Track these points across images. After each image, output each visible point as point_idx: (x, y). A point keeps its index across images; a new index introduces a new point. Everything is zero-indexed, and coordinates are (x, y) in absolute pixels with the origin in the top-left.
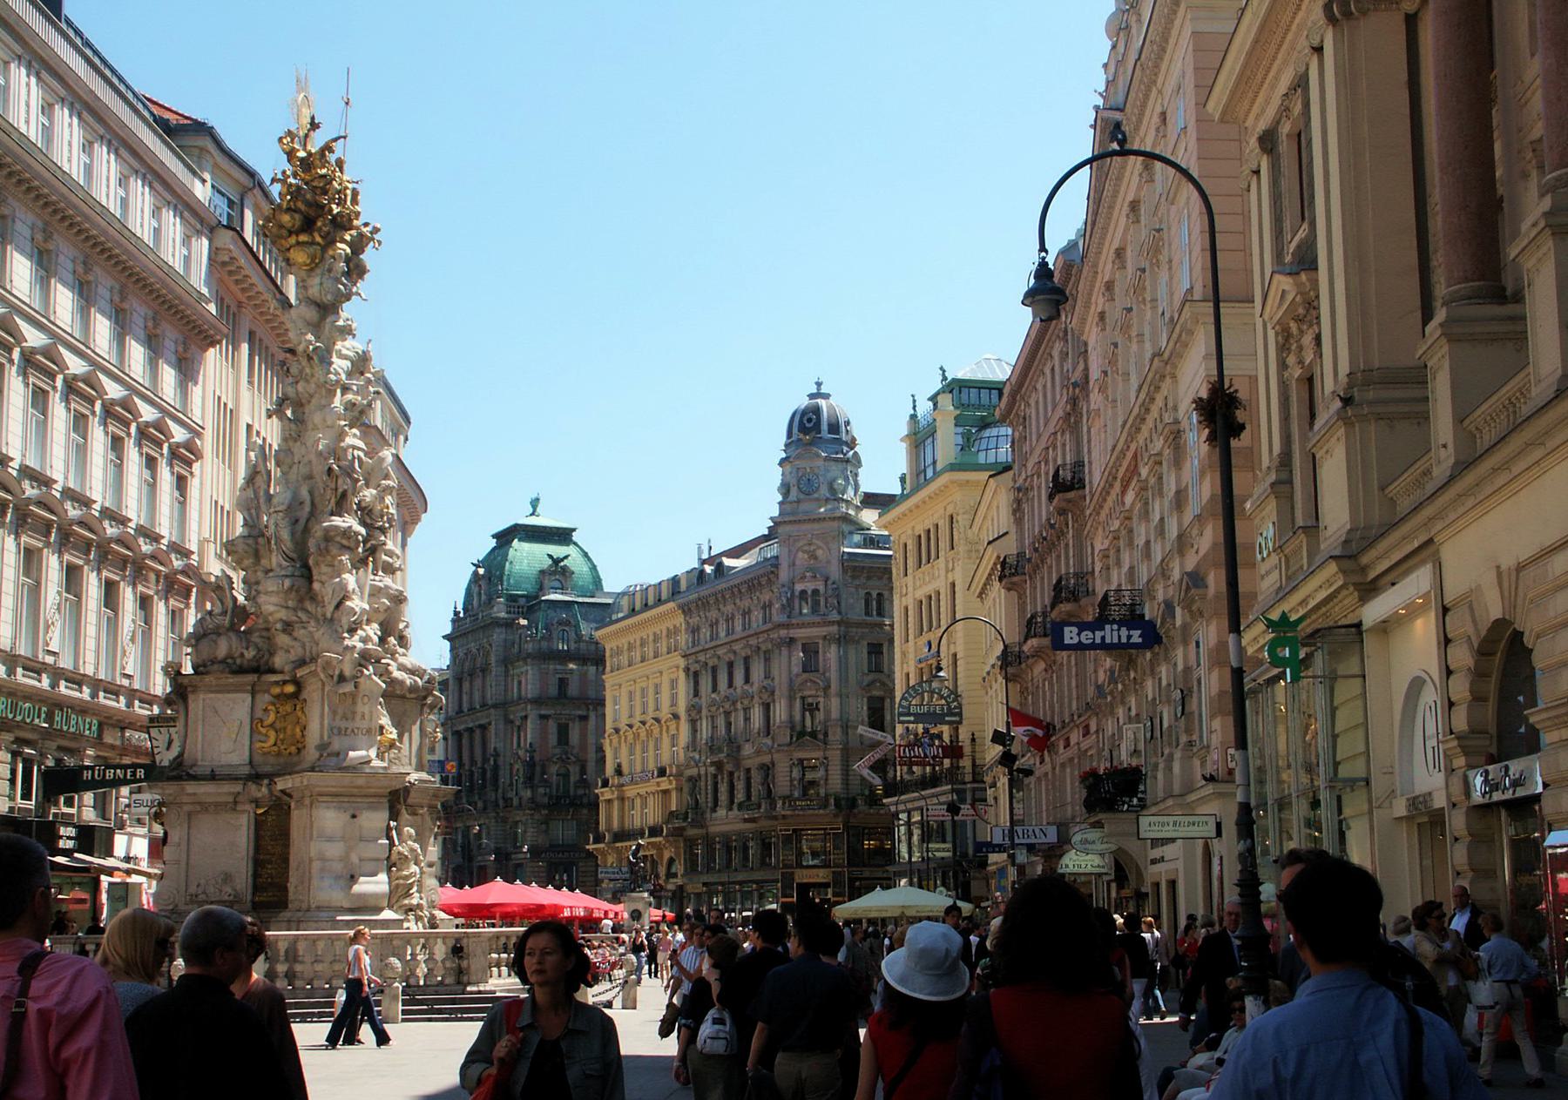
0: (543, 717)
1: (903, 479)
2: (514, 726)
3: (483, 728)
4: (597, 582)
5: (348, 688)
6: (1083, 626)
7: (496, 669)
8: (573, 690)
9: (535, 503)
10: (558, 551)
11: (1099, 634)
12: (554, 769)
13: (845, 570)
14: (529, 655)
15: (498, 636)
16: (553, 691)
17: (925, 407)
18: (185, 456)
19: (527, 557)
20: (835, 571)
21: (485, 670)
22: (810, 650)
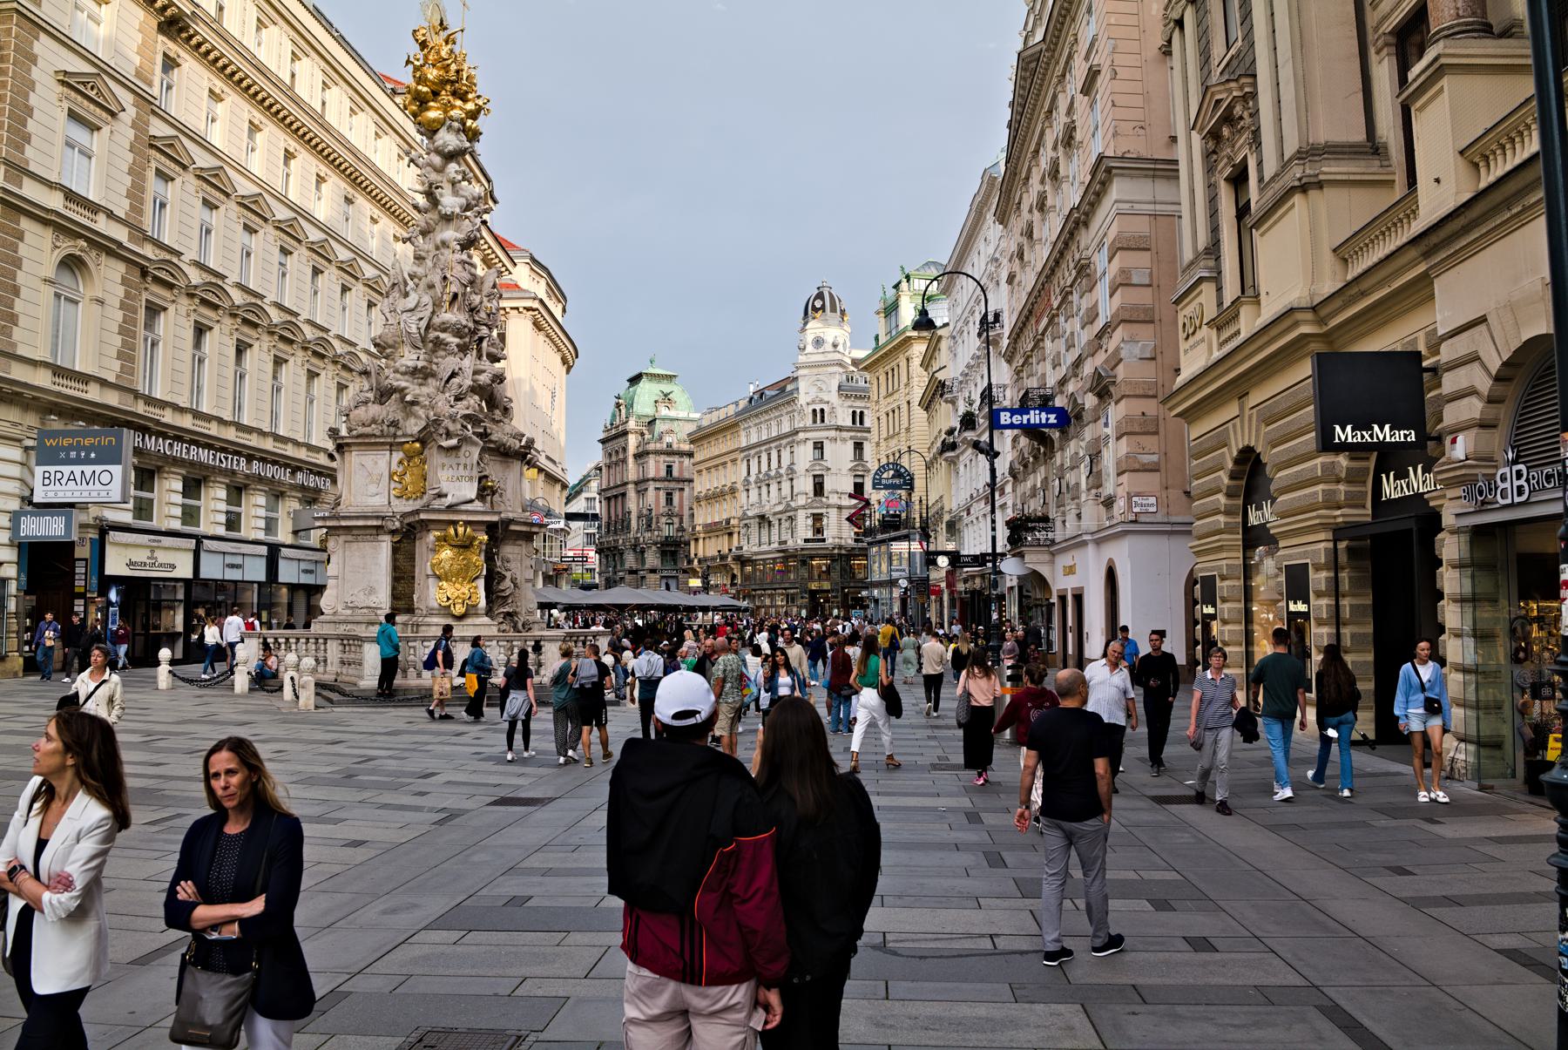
1: (877, 338)
2: (641, 492)
3: (624, 495)
6: (1013, 412)
7: (631, 460)
8: (675, 473)
10: (666, 387)
11: (1025, 417)
13: (840, 395)
16: (663, 473)
17: (891, 292)
20: (833, 397)
21: (624, 461)
22: (819, 446)
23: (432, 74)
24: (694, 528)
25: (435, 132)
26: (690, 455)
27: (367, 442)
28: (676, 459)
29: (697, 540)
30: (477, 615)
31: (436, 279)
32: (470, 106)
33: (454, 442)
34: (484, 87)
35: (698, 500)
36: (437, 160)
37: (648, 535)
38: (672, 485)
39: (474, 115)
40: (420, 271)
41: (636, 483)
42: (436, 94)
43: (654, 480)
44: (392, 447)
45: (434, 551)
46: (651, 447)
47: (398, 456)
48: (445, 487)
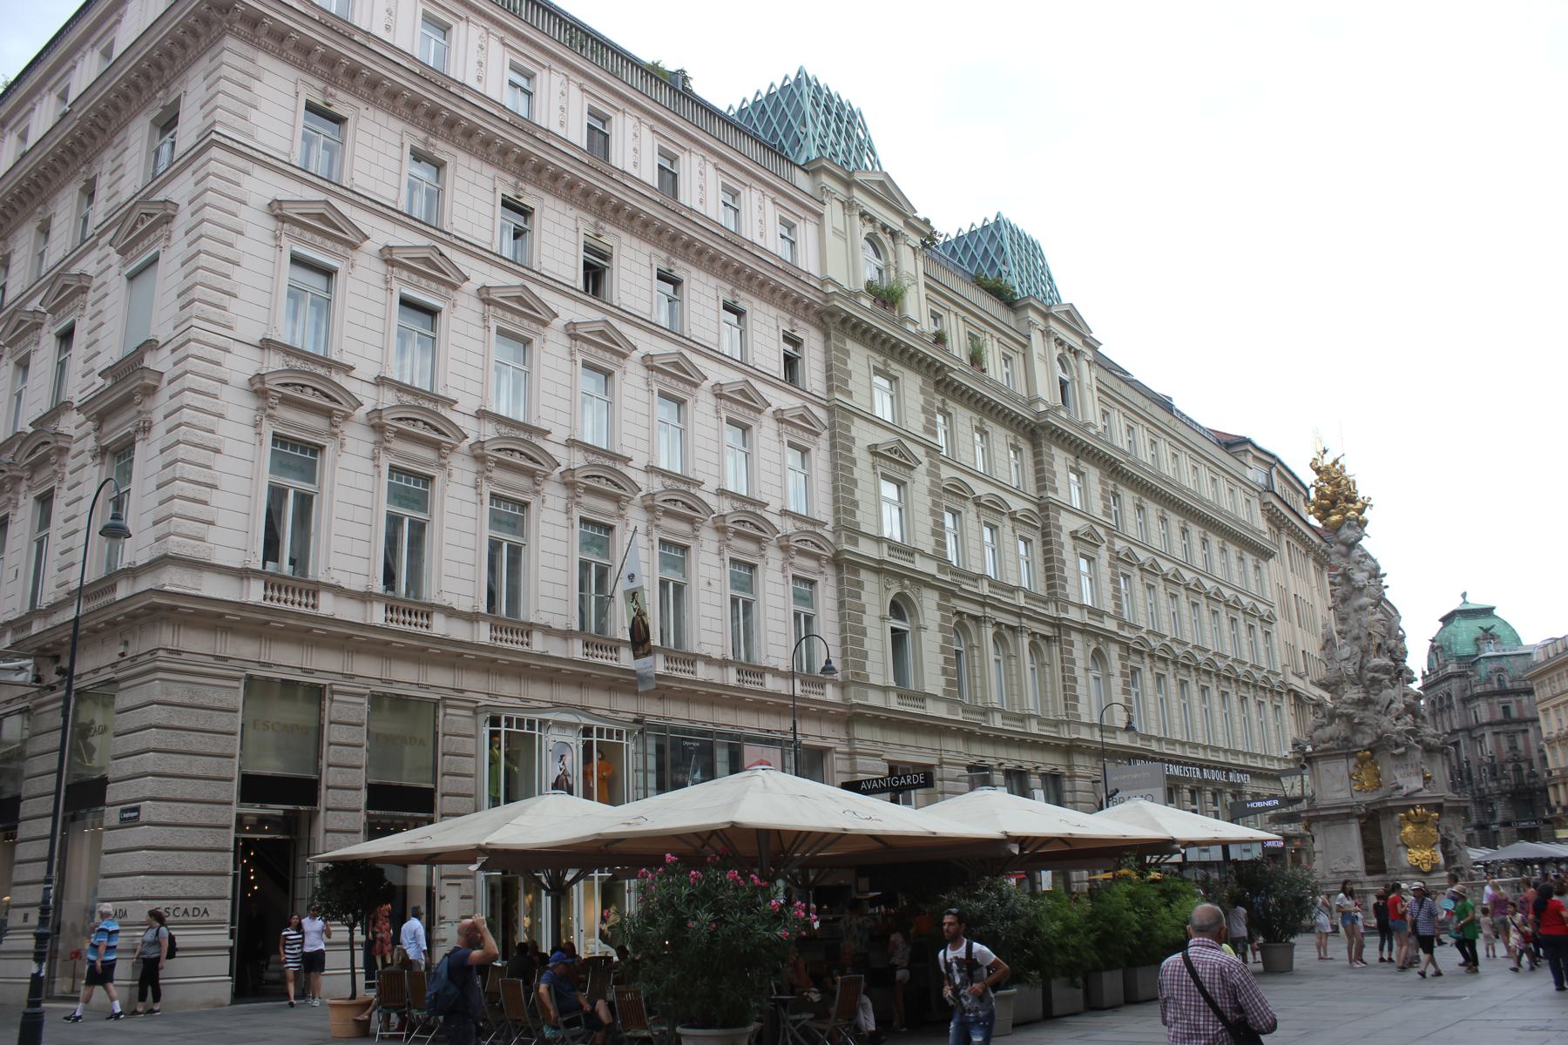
0: (1495, 733)
4: (1518, 640)
5: (1402, 750)
8: (1514, 713)
9: (1464, 595)
10: (1485, 622)
12: (1510, 766)
14: (1479, 696)
15: (1455, 685)
16: (1500, 716)
18: (1268, 620)
19: (1466, 631)
21: (1450, 707)
23: (1328, 490)
24: (1550, 773)
25: (1338, 529)
26: (1530, 692)
27: (1328, 755)
28: (1513, 699)
29: (1556, 786)
30: (1439, 871)
31: (1363, 635)
32: (1359, 505)
33: (1402, 750)
34: (1362, 492)
35: (1548, 741)
36: (1343, 549)
37: (1492, 785)
38: (1513, 727)
39: (1361, 511)
40: (1345, 628)
41: (1468, 730)
42: (1334, 503)
43: (1490, 724)
44: (1348, 756)
45: (1401, 828)
46: (1478, 689)
47: (1353, 761)
48: (1400, 781)
